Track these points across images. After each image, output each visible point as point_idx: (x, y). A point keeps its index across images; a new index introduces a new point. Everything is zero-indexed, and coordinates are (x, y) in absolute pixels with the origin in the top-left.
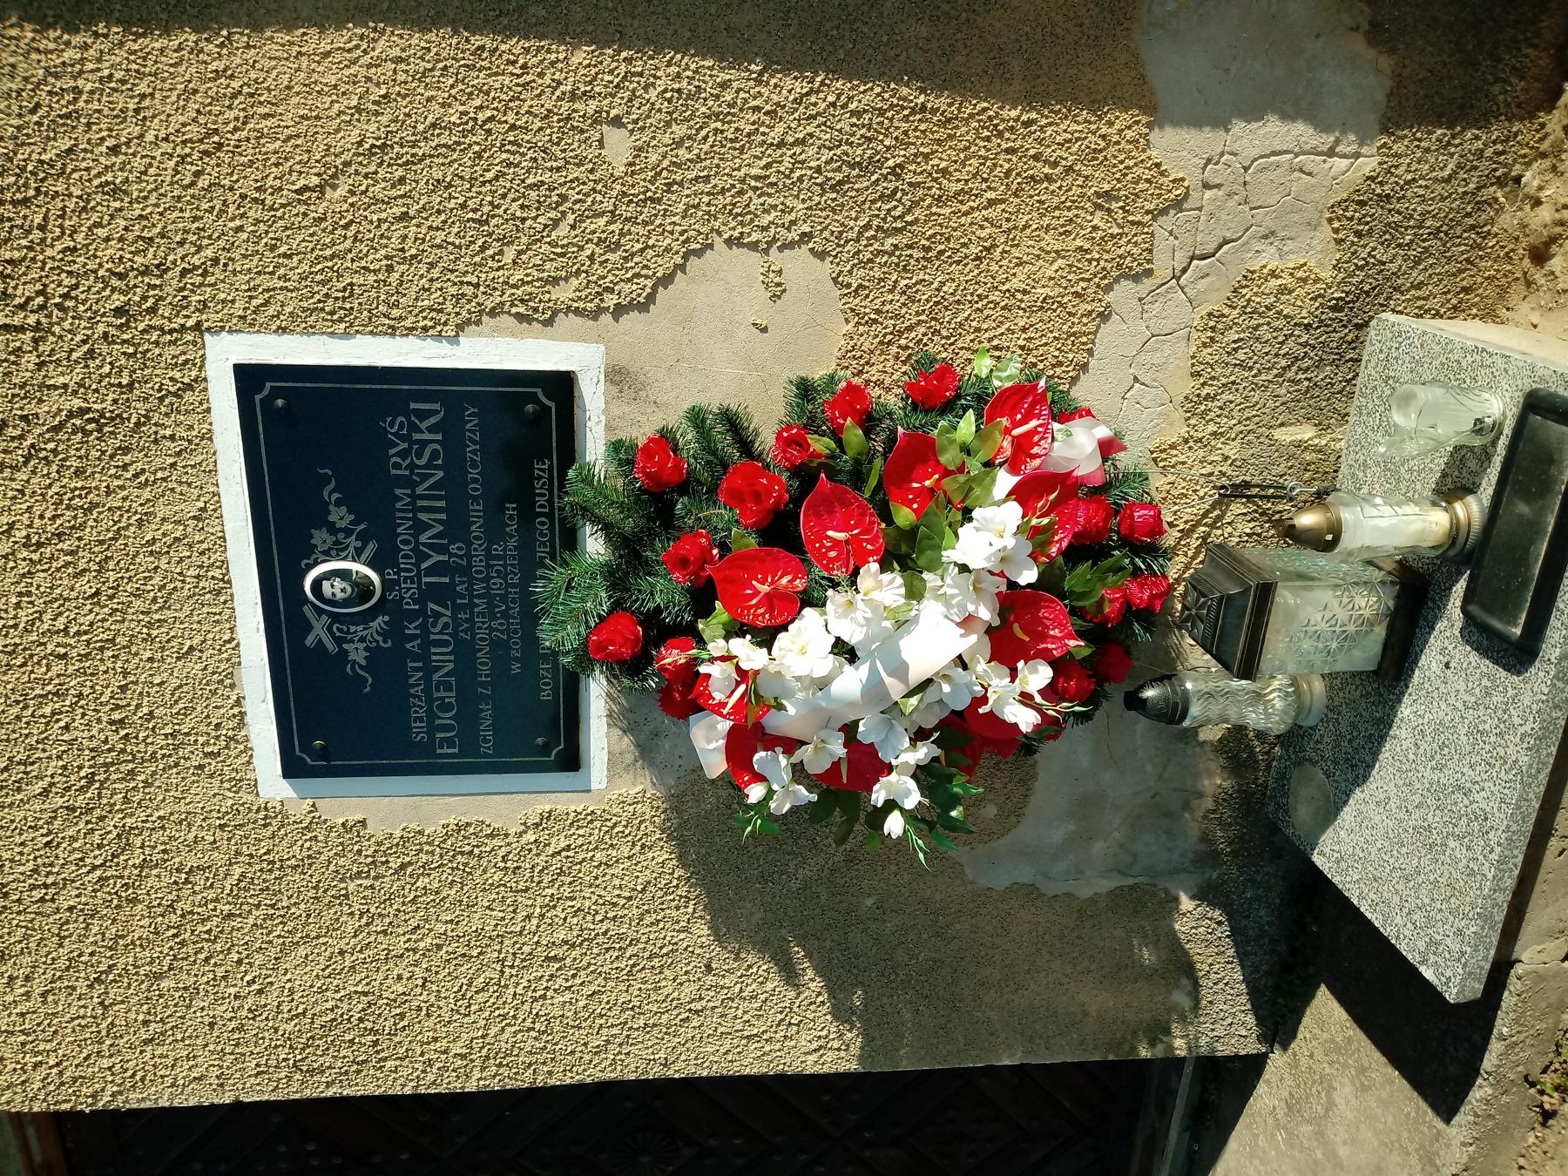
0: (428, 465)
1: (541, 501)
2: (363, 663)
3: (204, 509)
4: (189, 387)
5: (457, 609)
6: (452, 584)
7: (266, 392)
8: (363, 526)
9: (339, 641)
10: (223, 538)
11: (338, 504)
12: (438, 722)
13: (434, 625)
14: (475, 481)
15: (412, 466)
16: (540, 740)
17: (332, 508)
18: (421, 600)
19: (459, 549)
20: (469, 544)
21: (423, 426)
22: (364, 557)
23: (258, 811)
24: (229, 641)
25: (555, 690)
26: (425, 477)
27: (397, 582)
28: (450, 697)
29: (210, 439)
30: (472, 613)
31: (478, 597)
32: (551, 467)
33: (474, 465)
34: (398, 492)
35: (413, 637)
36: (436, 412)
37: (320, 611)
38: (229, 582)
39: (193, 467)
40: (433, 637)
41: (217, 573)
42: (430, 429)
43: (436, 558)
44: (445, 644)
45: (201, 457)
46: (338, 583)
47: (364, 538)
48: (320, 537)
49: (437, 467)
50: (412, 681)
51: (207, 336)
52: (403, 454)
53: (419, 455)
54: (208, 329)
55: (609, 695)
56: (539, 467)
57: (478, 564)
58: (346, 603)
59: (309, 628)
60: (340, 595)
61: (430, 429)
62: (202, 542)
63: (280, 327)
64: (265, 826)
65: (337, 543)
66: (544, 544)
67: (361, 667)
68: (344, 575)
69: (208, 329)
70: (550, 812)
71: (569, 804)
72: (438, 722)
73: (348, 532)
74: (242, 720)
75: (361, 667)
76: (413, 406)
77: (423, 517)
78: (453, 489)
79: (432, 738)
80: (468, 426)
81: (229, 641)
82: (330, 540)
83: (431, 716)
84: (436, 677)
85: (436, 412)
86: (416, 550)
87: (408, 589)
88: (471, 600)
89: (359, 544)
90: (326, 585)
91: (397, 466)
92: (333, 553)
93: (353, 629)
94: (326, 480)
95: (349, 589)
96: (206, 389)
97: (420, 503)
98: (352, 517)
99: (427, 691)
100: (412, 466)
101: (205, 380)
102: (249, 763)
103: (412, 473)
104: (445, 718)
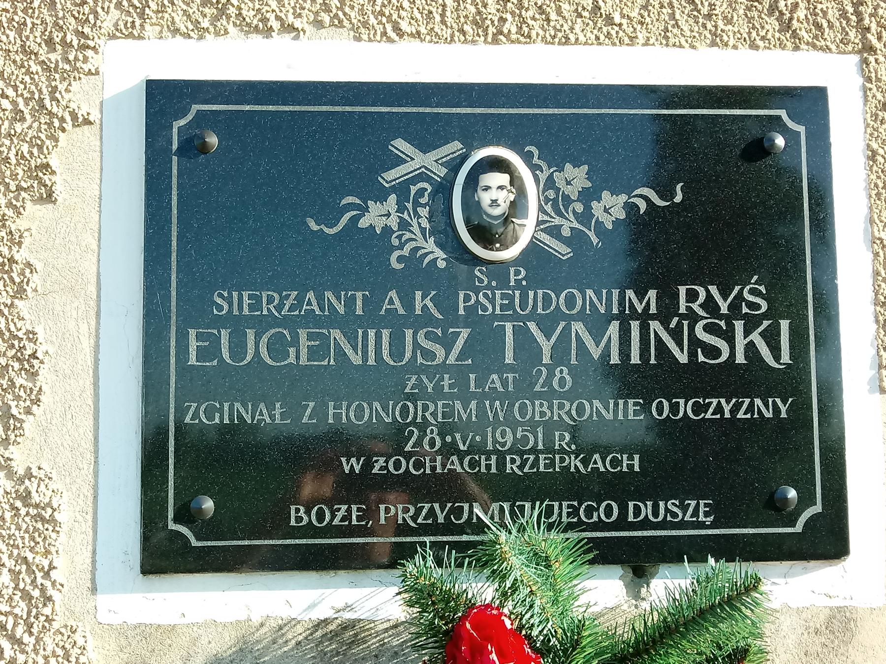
0: (695, 342)
1: (647, 510)
2: (363, 223)
3: (609, 21)
4: (786, 26)
5: (460, 373)
6: (502, 368)
7: (791, 124)
8: (595, 240)
9: (402, 190)
10: (566, 41)
11: (631, 208)
12: (251, 334)
13: (714, 352)
14: (674, 408)
15: (693, 318)
16: (208, 504)
17: (623, 198)
18: (472, 317)
19: (562, 380)
20: (571, 396)
21: (755, 337)
22: (545, 237)
23: (81, 34)
24: (397, 29)
25: (310, 531)
26: (677, 335)
27: (504, 283)
28: (300, 354)
29: (713, 44)
30: (451, 396)
31: (480, 408)
32: (701, 525)
33: (699, 409)
34: (652, 294)
35: (409, 304)
36: (777, 358)
37: (454, 166)
38: (495, 41)
39: (672, 16)
40: (409, 333)
41: (510, 26)
42: (751, 347)
43: (546, 346)
44: (397, 350)
45: (686, 28)
46: (505, 198)
47: (576, 240)
48: (575, 178)
49: (692, 355)
50: (329, 294)
51: (856, 58)
52: (710, 305)
53: (709, 329)
54: (865, 62)
55: (293, 622)
56: (699, 509)
57: (538, 409)
58: (471, 206)
59: (425, 147)
60: (486, 198)
61: (751, 347)
62: (559, 12)
63: (874, 153)
64: (50, 42)
65: (567, 200)
66: (575, 512)
67: (355, 220)
68: (517, 207)
69: (865, 62)
70: (53, 521)
71: (69, 557)
72: (251, 334)
73: (585, 217)
74: (256, 29)
75: (355, 220)
76: (784, 324)
77: (614, 328)
78: (704, 379)
79: (219, 322)
80: (758, 402)
81: (397, 29)
82: (572, 192)
83: (261, 324)
84: (336, 334)
85: (777, 358)
86: (558, 315)
87: (492, 301)
88: (474, 395)
89: (566, 232)
90: (503, 179)
91: (692, 296)
92: (551, 194)
93: (424, 212)
94: (666, 193)
95: (497, 212)
96: (783, 47)
97: (635, 325)
98: (610, 227)
99: (310, 319)
100: (693, 318)
101: (796, 48)
102: (176, 31)
103: (682, 317)
104: (256, 346)
